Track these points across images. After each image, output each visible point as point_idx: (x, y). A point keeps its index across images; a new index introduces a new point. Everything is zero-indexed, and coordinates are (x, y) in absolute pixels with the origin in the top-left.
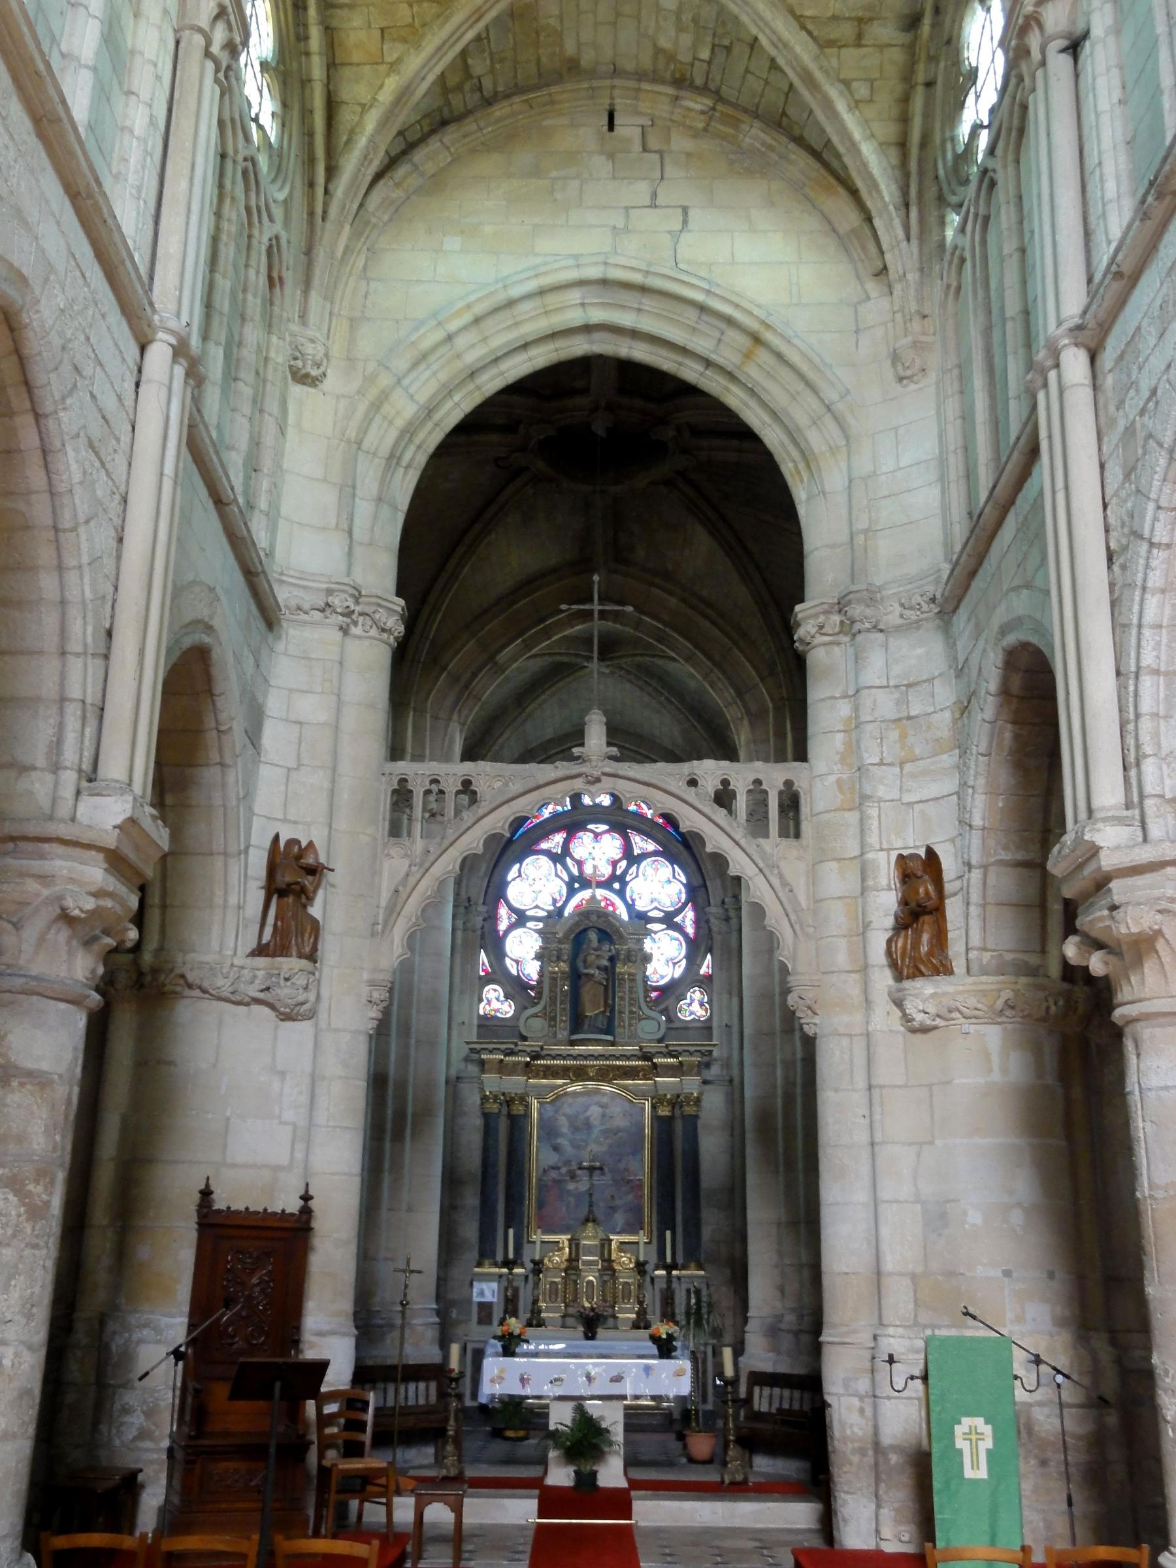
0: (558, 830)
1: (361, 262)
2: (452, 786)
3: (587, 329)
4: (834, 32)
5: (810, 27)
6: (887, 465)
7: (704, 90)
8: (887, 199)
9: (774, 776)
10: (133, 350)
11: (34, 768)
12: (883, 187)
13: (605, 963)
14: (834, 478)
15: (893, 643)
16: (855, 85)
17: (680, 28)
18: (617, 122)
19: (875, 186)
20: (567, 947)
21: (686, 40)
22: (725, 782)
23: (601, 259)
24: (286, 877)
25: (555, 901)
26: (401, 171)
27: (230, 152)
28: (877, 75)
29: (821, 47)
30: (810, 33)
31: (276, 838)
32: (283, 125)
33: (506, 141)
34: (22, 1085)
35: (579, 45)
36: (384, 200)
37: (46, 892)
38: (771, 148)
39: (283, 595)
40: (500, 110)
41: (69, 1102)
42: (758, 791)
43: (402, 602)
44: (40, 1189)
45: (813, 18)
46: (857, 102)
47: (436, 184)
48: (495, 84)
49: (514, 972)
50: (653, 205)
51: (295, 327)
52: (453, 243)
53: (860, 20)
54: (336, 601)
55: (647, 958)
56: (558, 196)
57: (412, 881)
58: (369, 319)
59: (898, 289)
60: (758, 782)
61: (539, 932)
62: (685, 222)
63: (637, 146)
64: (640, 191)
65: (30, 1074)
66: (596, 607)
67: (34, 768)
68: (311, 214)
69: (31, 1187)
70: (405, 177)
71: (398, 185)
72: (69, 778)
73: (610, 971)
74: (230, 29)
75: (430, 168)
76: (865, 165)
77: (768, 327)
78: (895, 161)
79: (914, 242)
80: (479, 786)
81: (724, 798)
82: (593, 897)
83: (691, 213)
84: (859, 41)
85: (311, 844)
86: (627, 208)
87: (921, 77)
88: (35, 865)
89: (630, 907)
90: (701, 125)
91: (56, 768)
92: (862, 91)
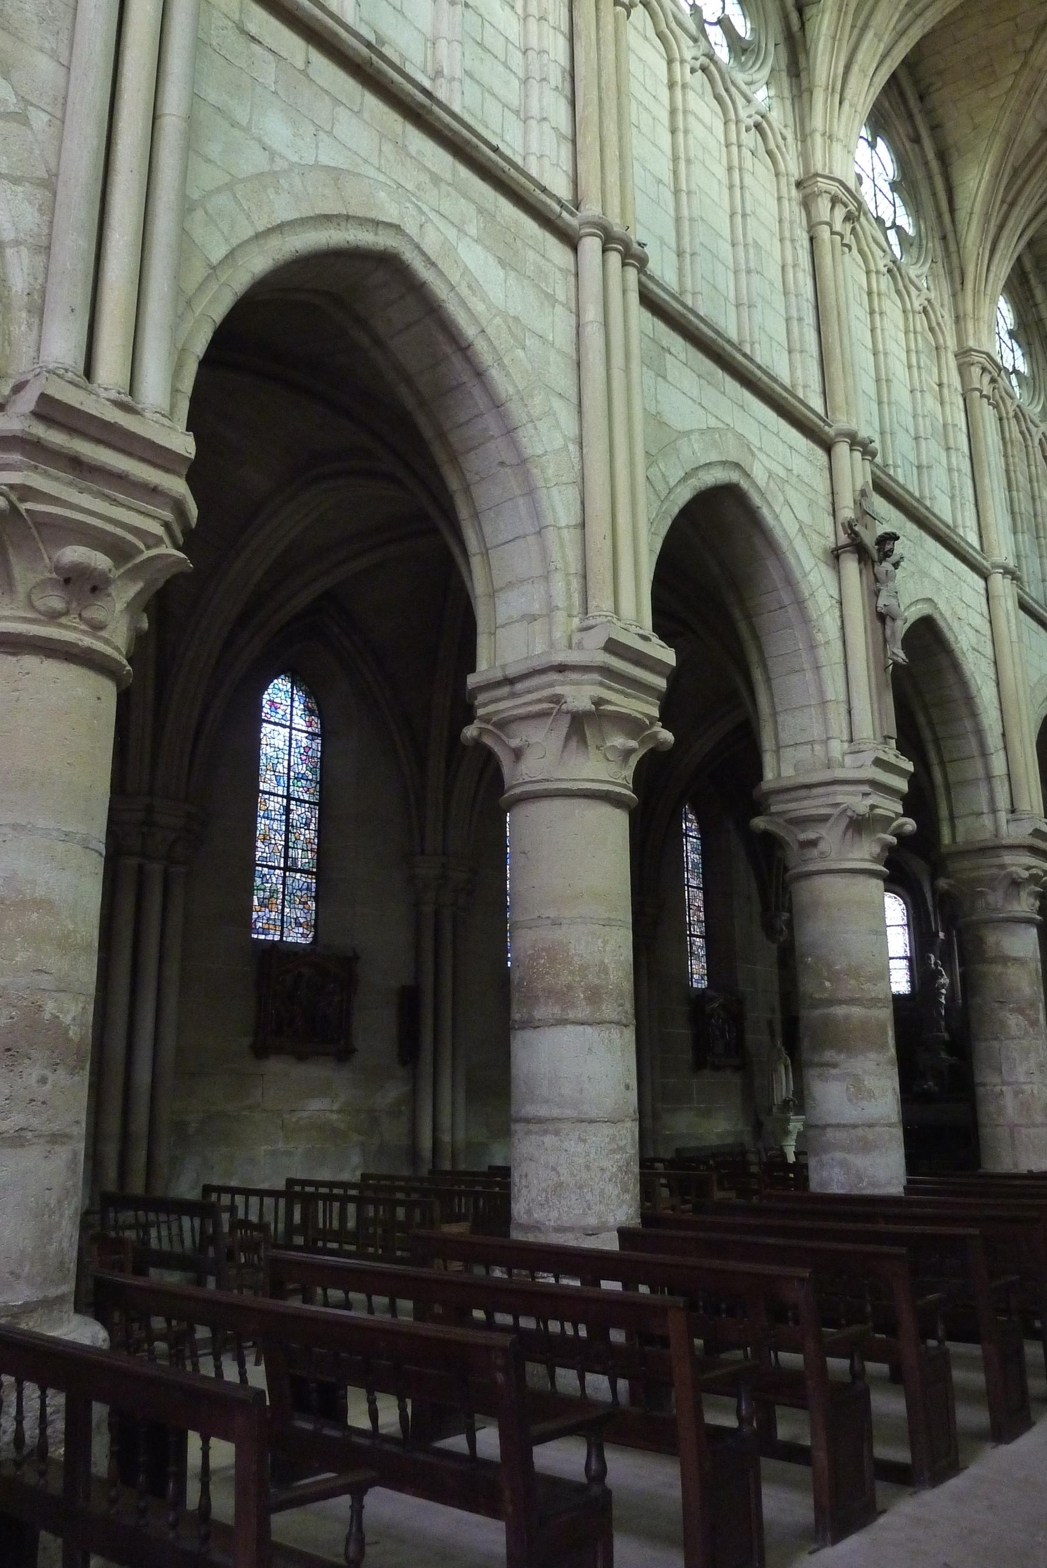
10: (982, 583)
11: (983, 813)
27: (1004, 415)
32: (1031, 356)
34: (1013, 964)
37: (1003, 873)
41: (1037, 970)
44: (1032, 1012)
65: (1016, 960)
67: (983, 813)
69: (1027, 1012)
72: (1003, 816)
74: (990, 373)
88: (996, 861)
91: (994, 811)
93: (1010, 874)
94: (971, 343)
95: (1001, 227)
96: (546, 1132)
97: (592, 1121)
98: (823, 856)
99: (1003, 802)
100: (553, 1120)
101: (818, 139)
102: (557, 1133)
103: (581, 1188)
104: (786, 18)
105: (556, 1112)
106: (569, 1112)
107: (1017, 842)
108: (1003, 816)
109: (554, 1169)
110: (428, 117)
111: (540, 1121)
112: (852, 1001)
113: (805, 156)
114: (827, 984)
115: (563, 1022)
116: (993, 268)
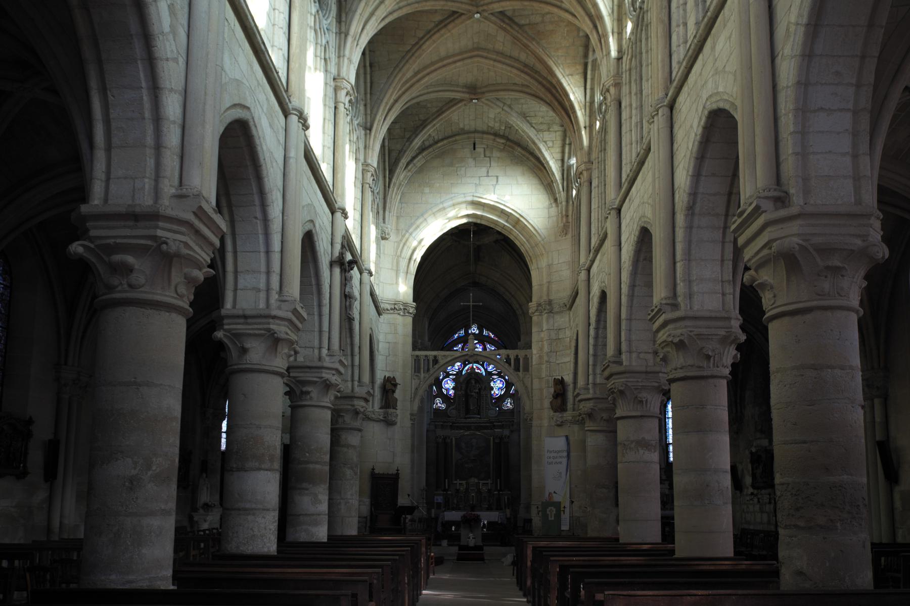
1: (399, 197)
3: (468, 216)
5: (534, 126)
6: (556, 262)
7: (502, 137)
12: (556, 174)
13: (477, 391)
14: (543, 263)
16: (548, 142)
17: (495, 122)
19: (553, 174)
20: (464, 386)
21: (497, 125)
24: (389, 386)
25: (459, 369)
26: (410, 167)
28: (554, 139)
29: (537, 132)
30: (534, 128)
33: (441, 155)
35: (464, 125)
36: (405, 176)
37: (353, 408)
38: (524, 155)
39: (382, 306)
40: (439, 145)
42: (517, 359)
43: (415, 304)
45: (535, 123)
46: (549, 147)
47: (421, 170)
48: (438, 137)
49: (445, 393)
50: (488, 176)
51: (382, 225)
52: (427, 190)
53: (549, 124)
55: (492, 389)
56: (459, 173)
57: (421, 385)
60: (517, 356)
61: (453, 379)
62: (497, 181)
63: (483, 156)
64: (484, 170)
66: (471, 304)
68: (385, 186)
70: (411, 168)
71: (409, 171)
72: (356, 383)
73: (479, 393)
75: (419, 165)
76: (550, 168)
78: (560, 165)
79: (565, 192)
80: (440, 358)
81: (508, 361)
82: (473, 367)
83: (500, 179)
84: (548, 130)
85: (394, 377)
86: (479, 177)
87: (567, 142)
90: (502, 148)
91: (353, 380)
92: (550, 144)
93: (356, 409)
94: (369, 161)
95: (390, 110)
98: (311, 398)
99: (356, 378)
101: (346, 60)
107: (360, 396)
108: (356, 383)
110: (262, 55)
115: (259, 469)
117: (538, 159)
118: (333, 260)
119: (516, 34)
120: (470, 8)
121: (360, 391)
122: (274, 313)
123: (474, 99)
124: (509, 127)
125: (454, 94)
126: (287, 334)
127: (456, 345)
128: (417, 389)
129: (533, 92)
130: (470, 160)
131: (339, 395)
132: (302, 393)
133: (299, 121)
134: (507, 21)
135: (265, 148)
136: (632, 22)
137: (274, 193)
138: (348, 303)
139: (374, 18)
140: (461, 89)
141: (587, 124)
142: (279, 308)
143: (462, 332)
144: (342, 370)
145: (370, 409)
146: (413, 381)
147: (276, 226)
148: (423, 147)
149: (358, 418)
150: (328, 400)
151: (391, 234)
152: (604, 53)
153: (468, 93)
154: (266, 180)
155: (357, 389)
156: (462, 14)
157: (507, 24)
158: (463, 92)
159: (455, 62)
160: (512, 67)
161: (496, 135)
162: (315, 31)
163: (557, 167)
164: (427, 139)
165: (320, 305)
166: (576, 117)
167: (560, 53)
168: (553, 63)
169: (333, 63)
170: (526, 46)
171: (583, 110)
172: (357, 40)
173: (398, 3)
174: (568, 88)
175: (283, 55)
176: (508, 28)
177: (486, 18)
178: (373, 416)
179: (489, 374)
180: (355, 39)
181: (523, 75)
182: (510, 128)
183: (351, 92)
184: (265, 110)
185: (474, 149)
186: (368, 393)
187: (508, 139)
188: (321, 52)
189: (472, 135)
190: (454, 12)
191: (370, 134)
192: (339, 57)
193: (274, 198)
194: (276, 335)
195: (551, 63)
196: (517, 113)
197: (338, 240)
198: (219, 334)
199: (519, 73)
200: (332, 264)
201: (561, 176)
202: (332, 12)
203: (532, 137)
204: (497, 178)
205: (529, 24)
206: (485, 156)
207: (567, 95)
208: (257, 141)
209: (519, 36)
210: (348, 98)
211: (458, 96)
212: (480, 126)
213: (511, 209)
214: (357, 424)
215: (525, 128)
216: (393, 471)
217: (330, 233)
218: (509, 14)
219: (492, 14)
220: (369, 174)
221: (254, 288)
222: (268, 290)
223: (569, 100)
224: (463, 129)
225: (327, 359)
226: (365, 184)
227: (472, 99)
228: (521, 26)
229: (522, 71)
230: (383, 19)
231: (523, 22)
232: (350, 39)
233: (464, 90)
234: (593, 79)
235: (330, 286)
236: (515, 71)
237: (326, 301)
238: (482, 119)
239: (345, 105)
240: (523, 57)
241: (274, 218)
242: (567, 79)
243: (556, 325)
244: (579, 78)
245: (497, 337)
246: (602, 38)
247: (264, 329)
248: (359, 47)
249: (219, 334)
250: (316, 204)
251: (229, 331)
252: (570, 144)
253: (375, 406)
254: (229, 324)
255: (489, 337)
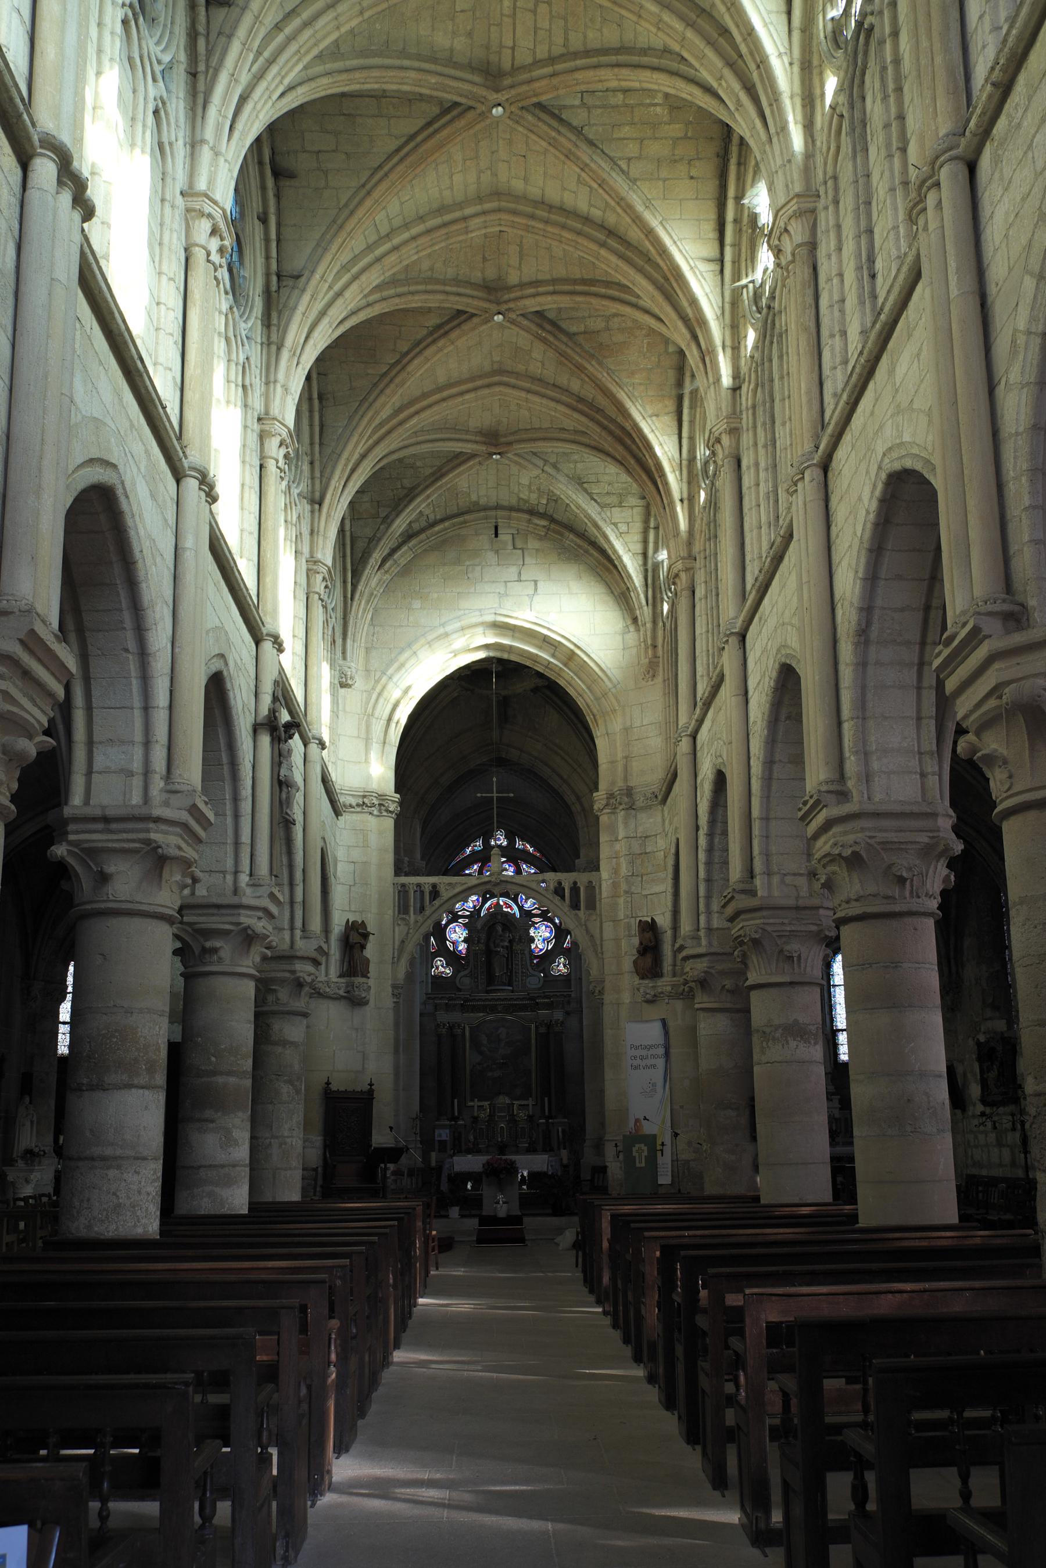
0: (476, 863)
1: (370, 616)
2: (427, 890)
3: (487, 647)
4: (608, 500)
6: (637, 723)
7: (543, 516)
8: (637, 585)
9: (582, 879)
12: (634, 578)
15: (639, 816)
17: (530, 491)
18: (499, 532)
19: (629, 577)
20: (483, 936)
22: (560, 883)
23: (493, 611)
25: (474, 907)
26: (388, 565)
29: (602, 507)
30: (595, 501)
31: (348, 921)
33: (440, 546)
35: (479, 497)
36: (380, 581)
38: (579, 546)
39: (342, 799)
40: (437, 528)
42: (575, 889)
43: (398, 796)
46: (621, 533)
47: (406, 571)
51: (341, 662)
52: (417, 604)
53: (620, 495)
54: (366, 800)
56: (470, 575)
58: (376, 648)
59: (642, 629)
60: (575, 883)
62: (536, 589)
64: (514, 570)
66: (495, 795)
68: (345, 597)
70: (390, 568)
71: (386, 572)
72: (298, 933)
75: (403, 562)
76: (625, 567)
77: (579, 647)
78: (641, 562)
79: (650, 607)
80: (442, 889)
81: (559, 891)
82: (498, 903)
83: (540, 584)
86: (506, 582)
87: (652, 525)
89: (521, 908)
91: (292, 928)
92: (623, 528)
93: (299, 978)
94: (319, 556)
96: (108, 1168)
97: (145, 1159)
98: (220, 960)
99: (298, 923)
100: (115, 1158)
101: (279, 390)
102: (119, 1167)
103: (134, 1207)
104: (267, 275)
105: (119, 1152)
106: (131, 1153)
107: (306, 955)
108: (298, 933)
109: (114, 1194)
111: (104, 1159)
112: (230, 1073)
113: (267, 398)
114: (213, 1059)
116: (341, 500)
117: (603, 552)
118: (258, 721)
119: (563, 347)
120: (486, 305)
121: (304, 947)
122: (157, 812)
123: (495, 454)
124: (554, 499)
125: (460, 444)
126: (180, 848)
127: (469, 865)
128: (403, 942)
129: (593, 443)
130: (491, 557)
131: (269, 953)
132: (205, 951)
133: (200, 489)
134: (548, 327)
135: (142, 532)
136: (755, 330)
137: (158, 609)
138: (284, 796)
139: (325, 321)
140: (473, 438)
141: (685, 496)
142: (166, 804)
143: (479, 845)
144: (274, 909)
145: (322, 978)
146: (397, 929)
147: (161, 665)
148: (410, 532)
149: (303, 993)
150: (249, 963)
151: (357, 678)
152: (711, 380)
153: (485, 443)
154: (144, 585)
155: (300, 943)
156: (473, 315)
157: (550, 332)
158: (476, 442)
159: (462, 394)
160: (558, 401)
161: (532, 512)
162: (227, 339)
163: (636, 564)
164: (416, 520)
165: (236, 799)
166: (666, 483)
167: (637, 379)
168: (625, 397)
169: (257, 394)
170: (580, 368)
171: (677, 473)
172: (297, 356)
173: (365, 296)
174: (651, 437)
175: (174, 378)
176: (551, 339)
177: (513, 322)
178: (328, 990)
179: (527, 915)
180: (294, 354)
181: (576, 415)
182: (556, 501)
183: (288, 441)
184: (143, 469)
185: (496, 535)
186: (320, 950)
187: (552, 520)
188: (237, 374)
189: (493, 513)
190: (460, 313)
191: (320, 510)
192: (267, 383)
193: (158, 616)
194: (160, 850)
195: (622, 396)
196: (567, 476)
197: (267, 688)
198: (60, 850)
199: (568, 411)
200: (256, 728)
201: (642, 580)
202: (255, 309)
203: (594, 516)
204: (536, 585)
205: (585, 333)
206: (515, 548)
207: (649, 447)
208: (130, 522)
209: (569, 351)
210: (283, 451)
211: (468, 448)
212: (506, 498)
213: (559, 635)
214: (300, 1004)
215: (580, 502)
216: (363, 1086)
217: (253, 676)
218: (551, 315)
219: (522, 315)
220: (319, 577)
221: (122, 770)
222: (147, 772)
223: (654, 455)
224: (476, 503)
225: (249, 891)
226: (311, 595)
227: (491, 454)
228: (571, 336)
229: (575, 409)
230: (341, 322)
231: (574, 329)
232: (285, 354)
233: (478, 438)
234: (692, 422)
235: (254, 767)
236: (561, 408)
237: (246, 791)
238: (509, 486)
239: (277, 462)
240: (575, 385)
241: (158, 651)
242: (650, 422)
243: (640, 829)
244: (669, 421)
245: (539, 851)
246: (707, 355)
247: (139, 841)
248: (300, 366)
249: (60, 850)
250: (229, 627)
251: (76, 844)
252: (657, 528)
253: (331, 973)
254: (77, 832)
255: (525, 851)
